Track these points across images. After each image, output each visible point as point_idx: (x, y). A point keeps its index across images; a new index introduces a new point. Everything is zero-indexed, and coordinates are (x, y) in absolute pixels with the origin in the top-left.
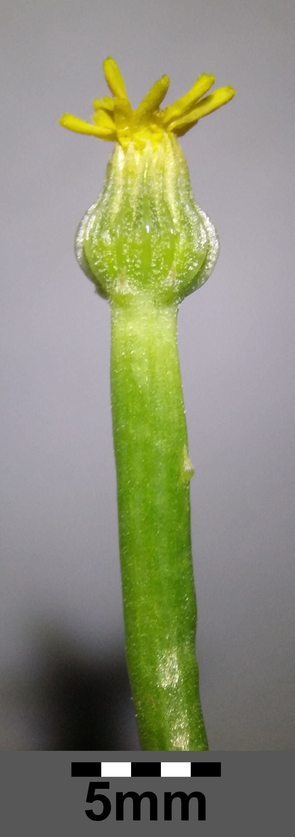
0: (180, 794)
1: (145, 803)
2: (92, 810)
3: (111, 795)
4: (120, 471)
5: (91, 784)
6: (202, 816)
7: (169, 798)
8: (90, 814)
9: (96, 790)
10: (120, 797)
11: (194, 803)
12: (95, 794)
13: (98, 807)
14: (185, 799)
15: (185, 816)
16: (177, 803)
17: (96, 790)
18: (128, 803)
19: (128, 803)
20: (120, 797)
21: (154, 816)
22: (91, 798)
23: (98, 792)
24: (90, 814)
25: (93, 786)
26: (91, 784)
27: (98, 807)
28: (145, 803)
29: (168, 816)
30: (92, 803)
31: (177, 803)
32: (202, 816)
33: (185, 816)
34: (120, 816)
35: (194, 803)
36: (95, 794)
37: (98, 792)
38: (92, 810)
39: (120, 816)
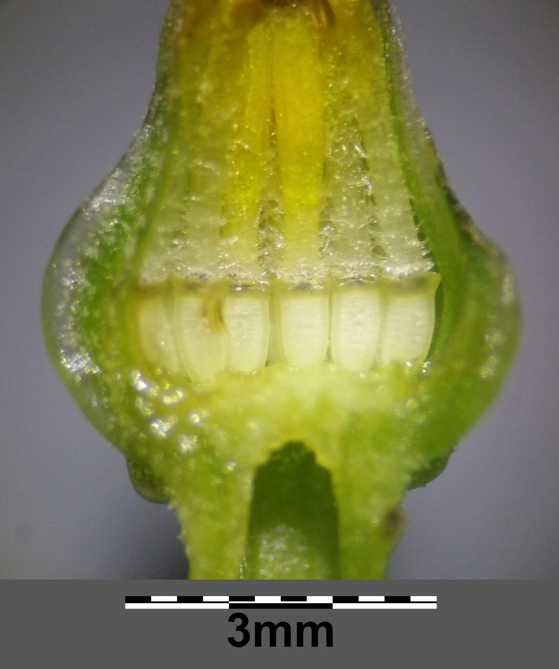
1: (280, 632)
2: (233, 638)
6: (330, 643)
7: (301, 627)
8: (232, 641)
11: (322, 632)
16: (308, 632)
19: (266, 632)
21: (288, 643)
24: (232, 641)
28: (280, 632)
29: (300, 643)
31: (308, 632)
32: (330, 643)
34: (258, 643)
35: (322, 632)
38: (233, 637)
39: (258, 643)
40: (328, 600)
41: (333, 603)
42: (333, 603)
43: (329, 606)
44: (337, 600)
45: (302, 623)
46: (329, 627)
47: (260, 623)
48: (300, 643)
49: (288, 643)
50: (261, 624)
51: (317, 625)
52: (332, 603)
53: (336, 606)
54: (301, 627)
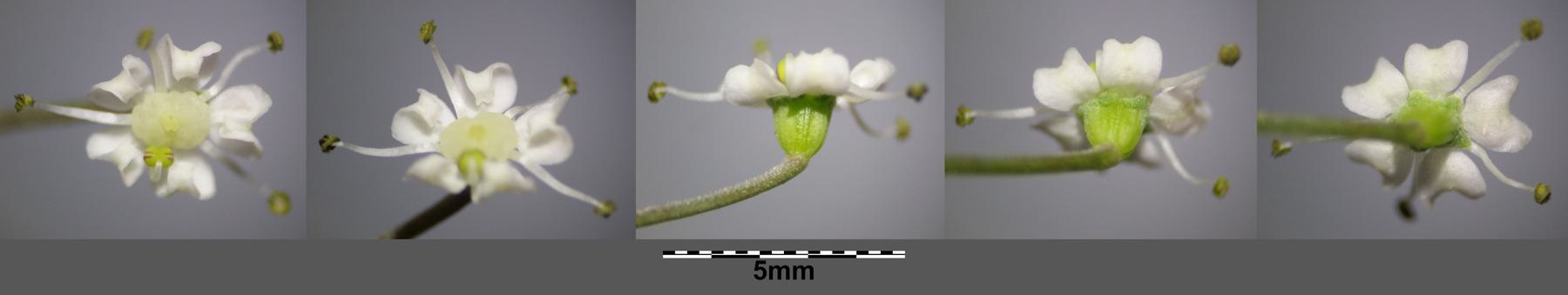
0: (801, 267)
1: (784, 271)
3: (767, 267)
4: (141, 89)
6: (812, 277)
7: (795, 268)
8: (756, 276)
10: (771, 268)
11: (808, 271)
13: (760, 273)
14: (803, 269)
15: (779, 278)
16: (799, 271)
20: (771, 268)
21: (788, 278)
22: (757, 269)
23: (760, 265)
24: (756, 276)
25: (758, 263)
27: (760, 273)
28: (784, 271)
29: (795, 278)
31: (799, 271)
32: (812, 277)
34: (771, 278)
35: (808, 271)
37: (760, 265)
39: (771, 278)
40: (854, 253)
43: (855, 256)
44: (859, 253)
46: (811, 268)
48: (795, 278)
49: (788, 278)
53: (858, 256)
54: (795, 268)
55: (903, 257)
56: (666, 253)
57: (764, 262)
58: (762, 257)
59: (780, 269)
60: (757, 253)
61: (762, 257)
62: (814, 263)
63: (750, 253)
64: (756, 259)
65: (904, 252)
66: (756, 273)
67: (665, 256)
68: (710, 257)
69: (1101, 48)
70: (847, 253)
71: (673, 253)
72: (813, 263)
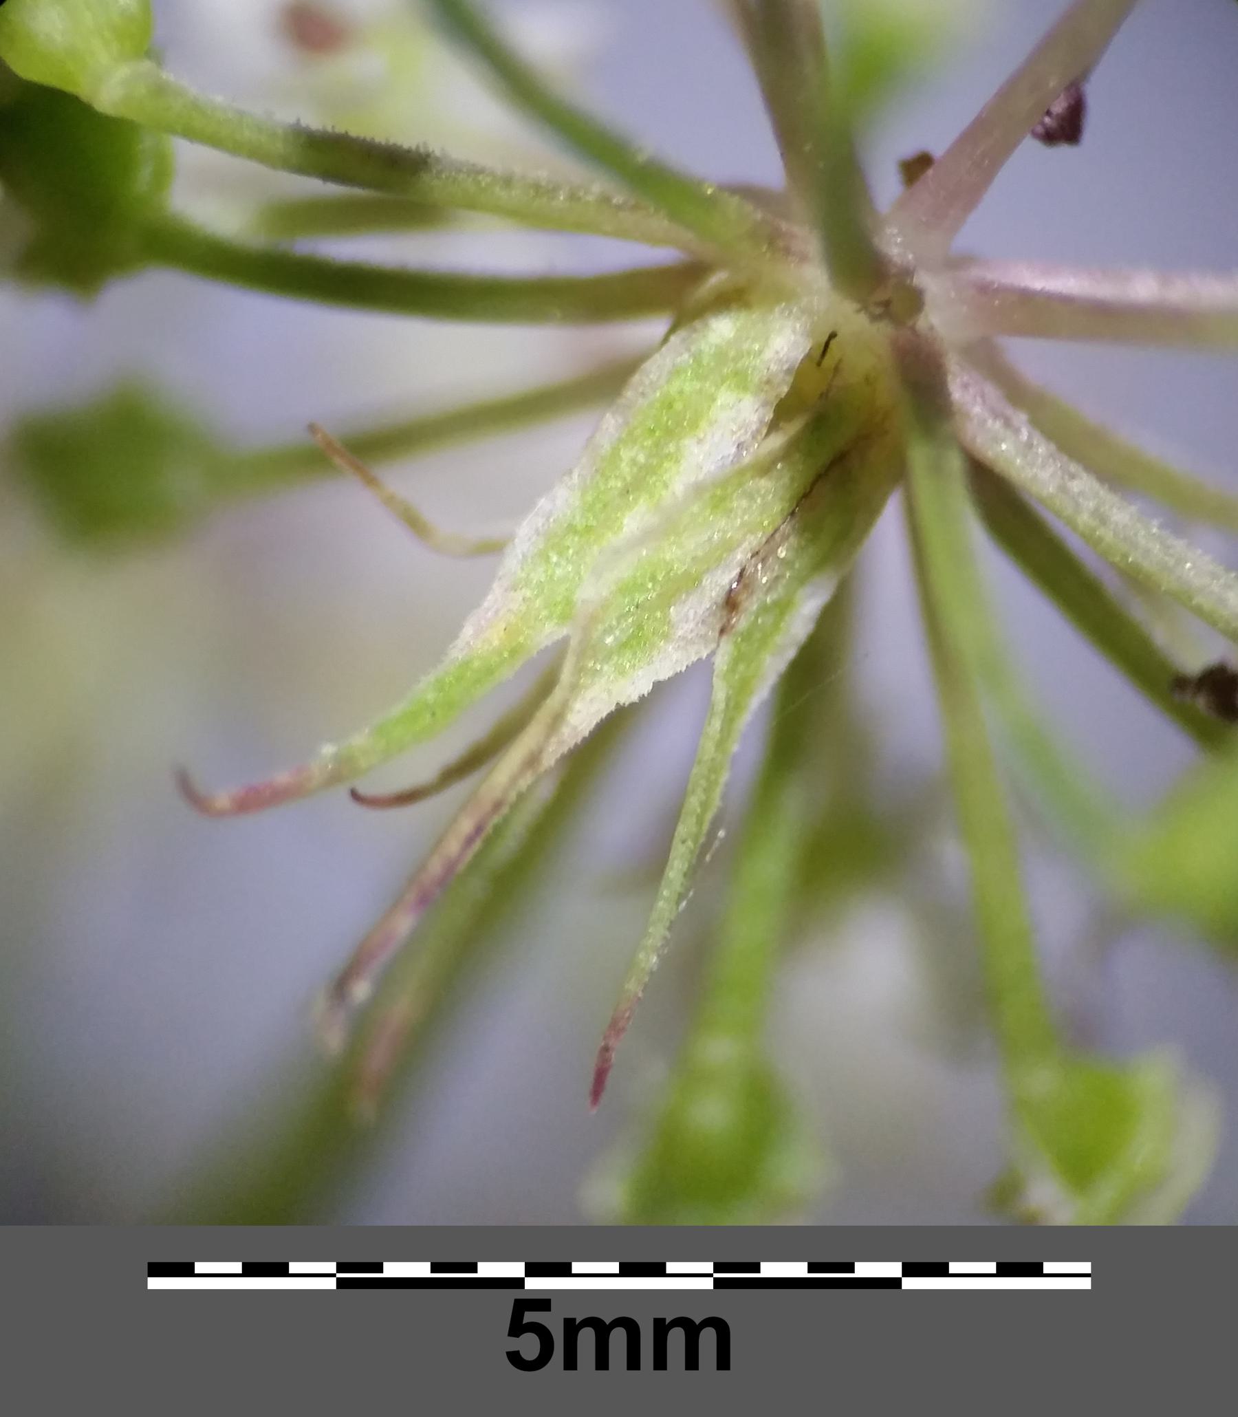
1: (618, 1339)
2: (518, 1352)
3: (553, 1322)
5: (516, 1301)
6: (723, 1362)
7: (662, 1328)
8: (515, 1358)
9: (527, 1314)
10: (571, 1328)
11: (708, 1338)
12: (524, 1323)
13: (529, 1346)
14: (692, 1330)
15: (602, 1362)
16: (676, 1339)
17: (527, 1314)
18: (587, 1338)
19: (587, 1338)
20: (571, 1328)
21: (633, 1362)
22: (517, 1328)
23: (529, 1317)
24: (515, 1358)
26: (516, 1301)
27: (529, 1346)
28: (618, 1339)
29: (660, 1362)
30: (518, 1336)
31: (676, 1339)
32: (723, 1362)
33: (692, 1362)
34: (570, 1362)
35: (708, 1338)
36: (524, 1323)
37: (529, 1317)
38: (518, 1352)
39: (570, 1362)
40: (892, 1269)
41: (903, 1276)
42: (903, 1276)
43: (895, 1283)
44: (909, 1270)
45: (664, 1320)
46: (721, 1327)
47: (575, 1319)
50: (577, 1322)
51: (697, 1323)
52: (903, 1279)
53: (909, 1283)
54: (662, 1328)
55: (1085, 1284)
56: (159, 1270)
57: (542, 1303)
58: (533, 1284)
59: (602, 1330)
60: (515, 1269)
61: (533, 1284)
62: (732, 1307)
63: (486, 1270)
64: (515, 1294)
65: (1086, 1267)
66: (515, 1344)
67: (155, 1283)
68: (331, 1284)
69: (1042, 290)
70: (864, 1270)
71: (187, 1270)
72: (732, 1307)
